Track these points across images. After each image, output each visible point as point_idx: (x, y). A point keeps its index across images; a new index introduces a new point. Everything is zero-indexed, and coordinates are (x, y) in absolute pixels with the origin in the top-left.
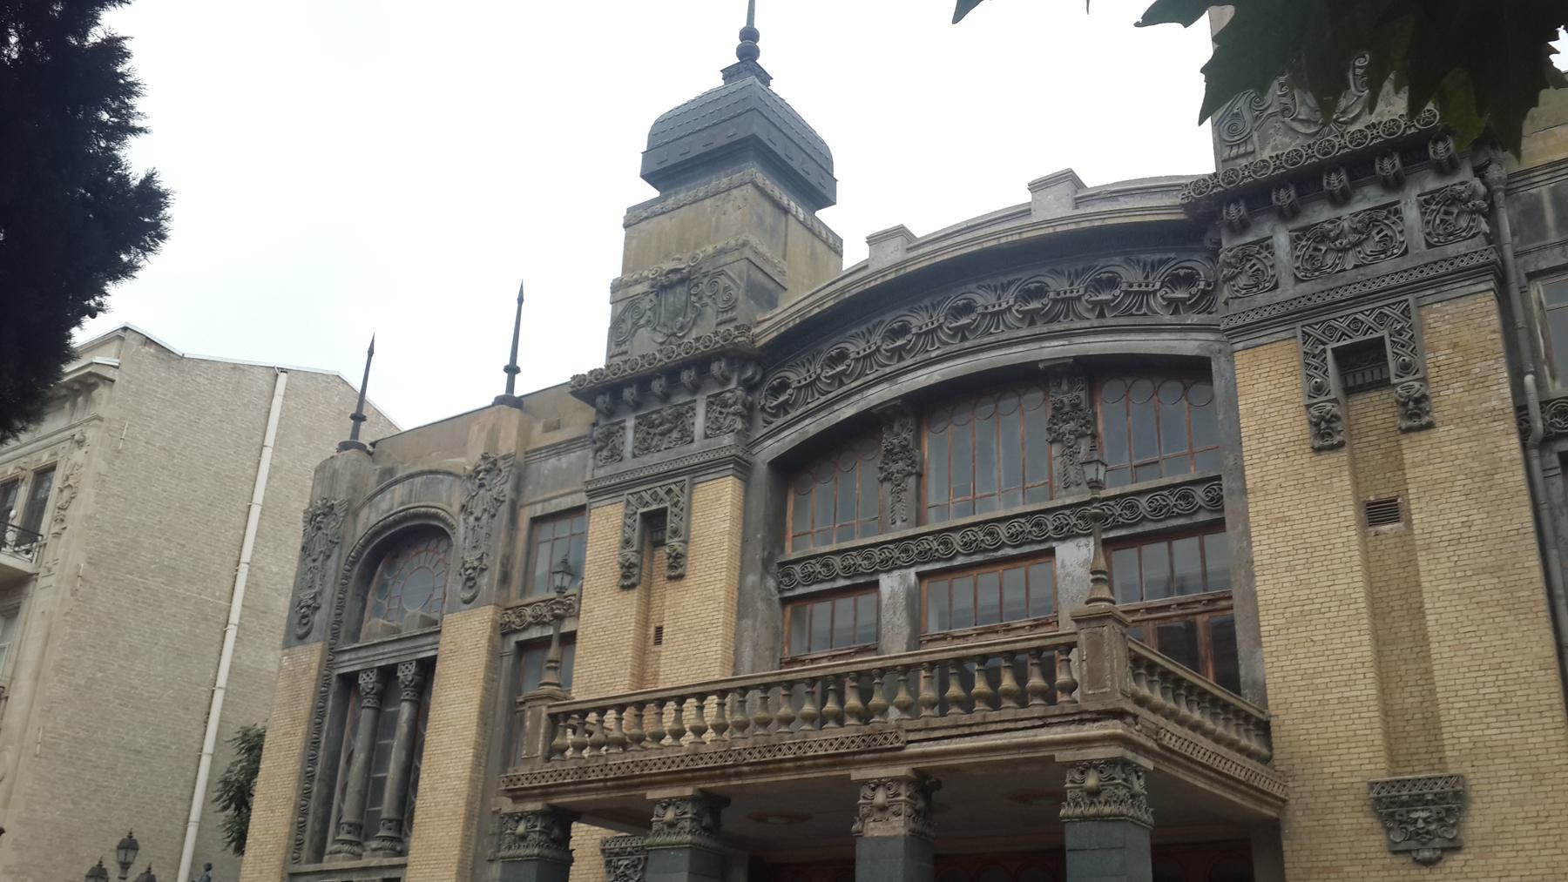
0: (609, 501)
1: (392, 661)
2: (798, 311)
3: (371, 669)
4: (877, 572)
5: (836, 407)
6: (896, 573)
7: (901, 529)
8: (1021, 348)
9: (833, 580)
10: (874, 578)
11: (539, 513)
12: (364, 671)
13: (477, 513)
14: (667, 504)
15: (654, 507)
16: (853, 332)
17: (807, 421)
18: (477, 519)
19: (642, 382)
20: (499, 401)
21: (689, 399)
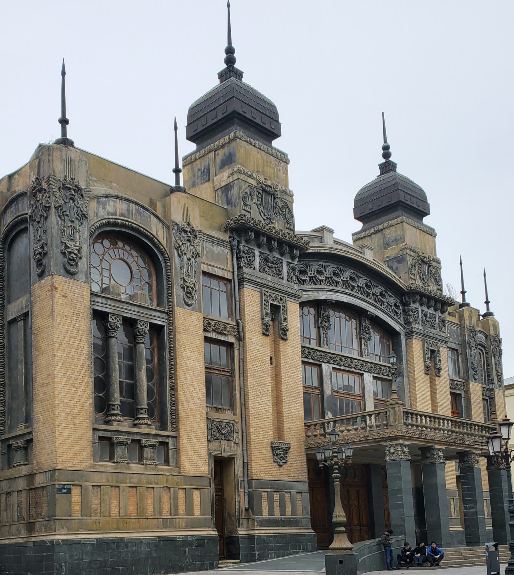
0: (252, 288)
1: (134, 317)
2: (319, 247)
3: (118, 316)
4: (323, 362)
5: (320, 292)
6: (327, 364)
7: (326, 348)
8: (361, 302)
9: (309, 359)
10: (320, 363)
11: (206, 270)
12: (113, 314)
13: (189, 256)
14: (280, 305)
15: (276, 303)
16: (321, 263)
17: (311, 292)
18: (189, 260)
19: (270, 238)
20: (58, 142)
21: (280, 257)
